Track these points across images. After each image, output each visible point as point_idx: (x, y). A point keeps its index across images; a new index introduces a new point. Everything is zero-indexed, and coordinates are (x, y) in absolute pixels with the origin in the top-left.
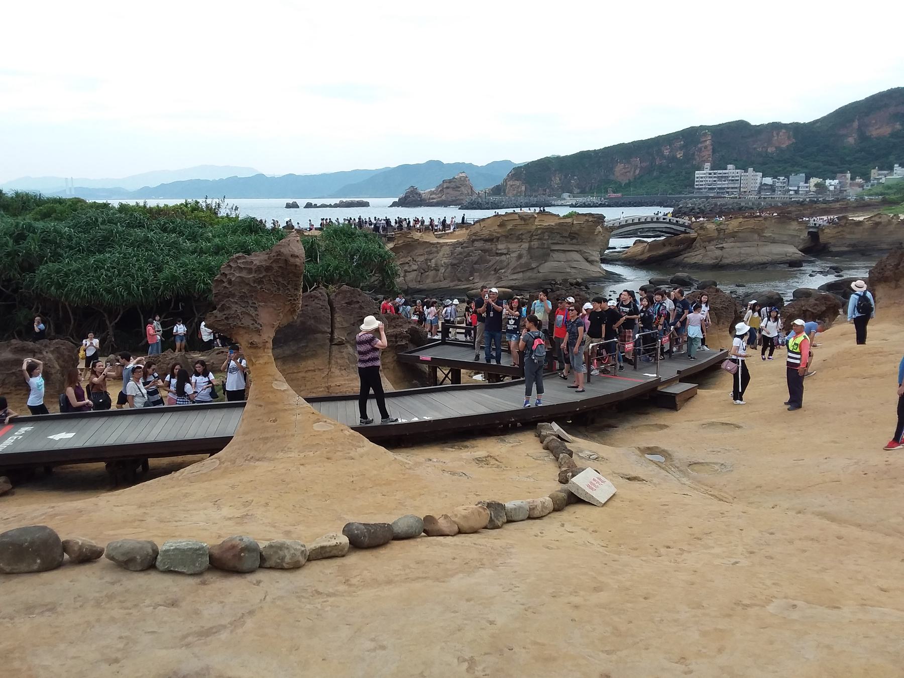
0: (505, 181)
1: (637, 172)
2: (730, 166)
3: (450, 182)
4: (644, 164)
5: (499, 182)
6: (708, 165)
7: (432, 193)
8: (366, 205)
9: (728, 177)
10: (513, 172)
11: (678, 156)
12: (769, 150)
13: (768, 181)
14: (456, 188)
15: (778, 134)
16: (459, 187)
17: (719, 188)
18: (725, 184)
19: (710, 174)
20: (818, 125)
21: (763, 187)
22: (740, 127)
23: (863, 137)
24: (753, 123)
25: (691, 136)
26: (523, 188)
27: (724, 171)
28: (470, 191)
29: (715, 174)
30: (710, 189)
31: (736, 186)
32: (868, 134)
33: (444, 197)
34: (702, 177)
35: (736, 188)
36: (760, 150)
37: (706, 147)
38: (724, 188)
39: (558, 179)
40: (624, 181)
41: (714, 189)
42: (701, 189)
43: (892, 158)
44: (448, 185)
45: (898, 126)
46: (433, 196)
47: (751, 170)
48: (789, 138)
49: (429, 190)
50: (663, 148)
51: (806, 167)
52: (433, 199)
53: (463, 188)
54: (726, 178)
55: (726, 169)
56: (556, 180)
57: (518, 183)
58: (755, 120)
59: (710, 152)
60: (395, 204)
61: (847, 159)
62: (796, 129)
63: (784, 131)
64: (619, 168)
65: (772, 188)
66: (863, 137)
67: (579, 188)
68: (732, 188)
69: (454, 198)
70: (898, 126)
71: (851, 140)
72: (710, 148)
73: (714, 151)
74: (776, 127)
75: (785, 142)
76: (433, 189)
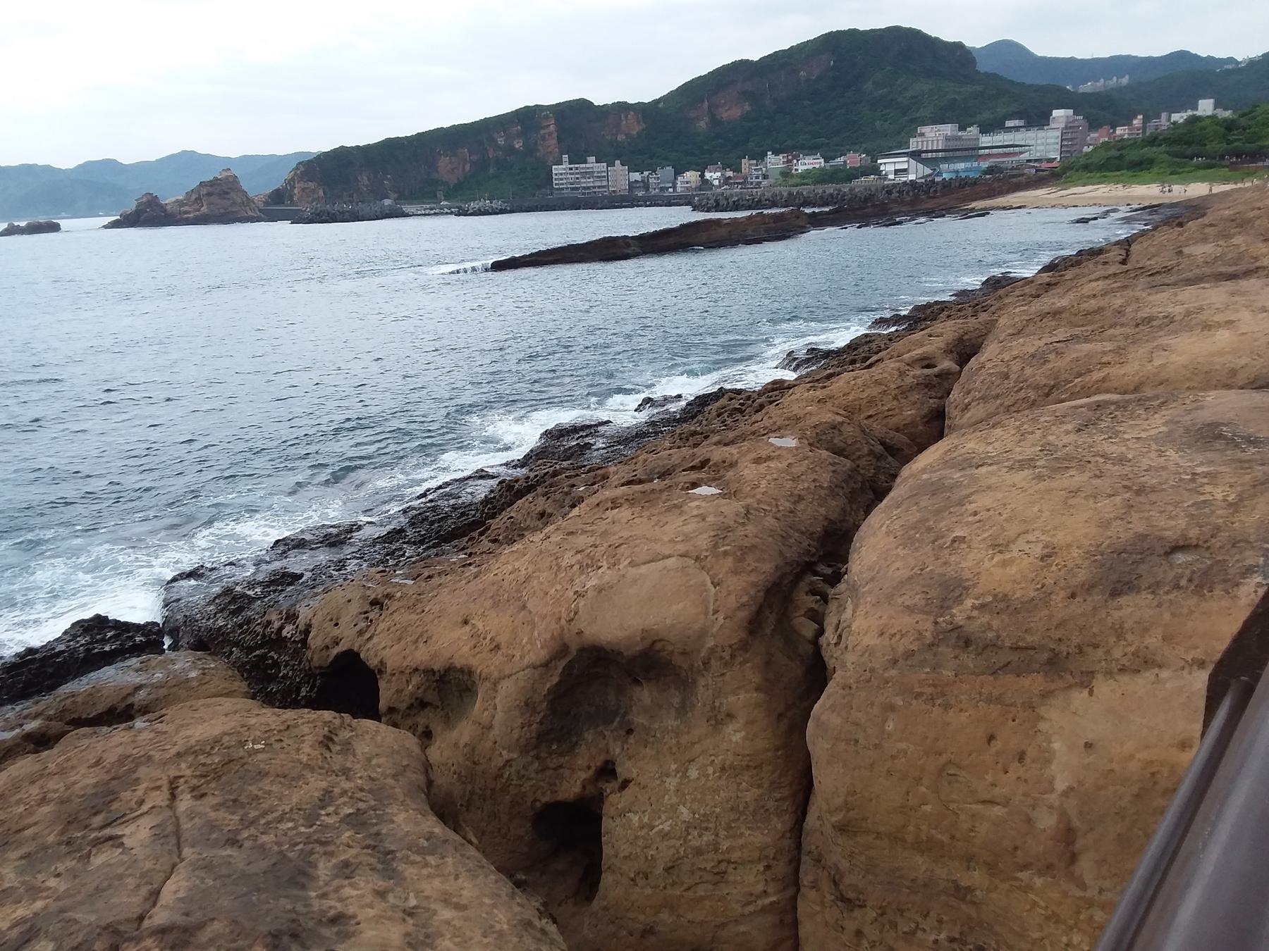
0: (291, 182)
1: (468, 167)
2: (592, 159)
3: (211, 186)
4: (474, 158)
5: (278, 183)
6: (565, 157)
7: (180, 203)
8: (55, 228)
9: (593, 172)
10: (302, 169)
11: (517, 146)
12: (620, 138)
13: (636, 176)
14: (224, 194)
15: (626, 117)
16: (228, 193)
17: (584, 188)
18: (590, 182)
19: (571, 169)
20: (661, 105)
21: (632, 185)
22: (580, 108)
23: (715, 122)
24: (596, 104)
25: (528, 117)
26: (321, 193)
27: (588, 165)
28: (245, 199)
29: (577, 169)
30: (573, 189)
31: (605, 183)
32: (718, 117)
33: (204, 209)
34: (561, 174)
35: (604, 187)
36: (609, 138)
37: (550, 134)
38: (588, 188)
39: (365, 178)
40: (453, 181)
41: (577, 189)
42: (563, 189)
43: (751, 145)
44: (210, 189)
45: (747, 107)
46: (186, 208)
47: (618, 162)
48: (638, 123)
49: (173, 199)
50: (496, 135)
51: (666, 159)
52: (186, 212)
53: (233, 195)
54: (586, 174)
55: (585, 162)
56: (364, 180)
57: (312, 185)
58: (601, 96)
59: (555, 141)
60: (115, 225)
61: (706, 147)
62: (640, 108)
63: (632, 113)
64: (444, 163)
65: (645, 185)
66: (715, 122)
67: (396, 192)
68: (599, 187)
69: (222, 211)
70: (747, 107)
71: (702, 124)
72: (555, 135)
73: (560, 140)
74: (621, 107)
75: (634, 127)
76: (181, 198)
